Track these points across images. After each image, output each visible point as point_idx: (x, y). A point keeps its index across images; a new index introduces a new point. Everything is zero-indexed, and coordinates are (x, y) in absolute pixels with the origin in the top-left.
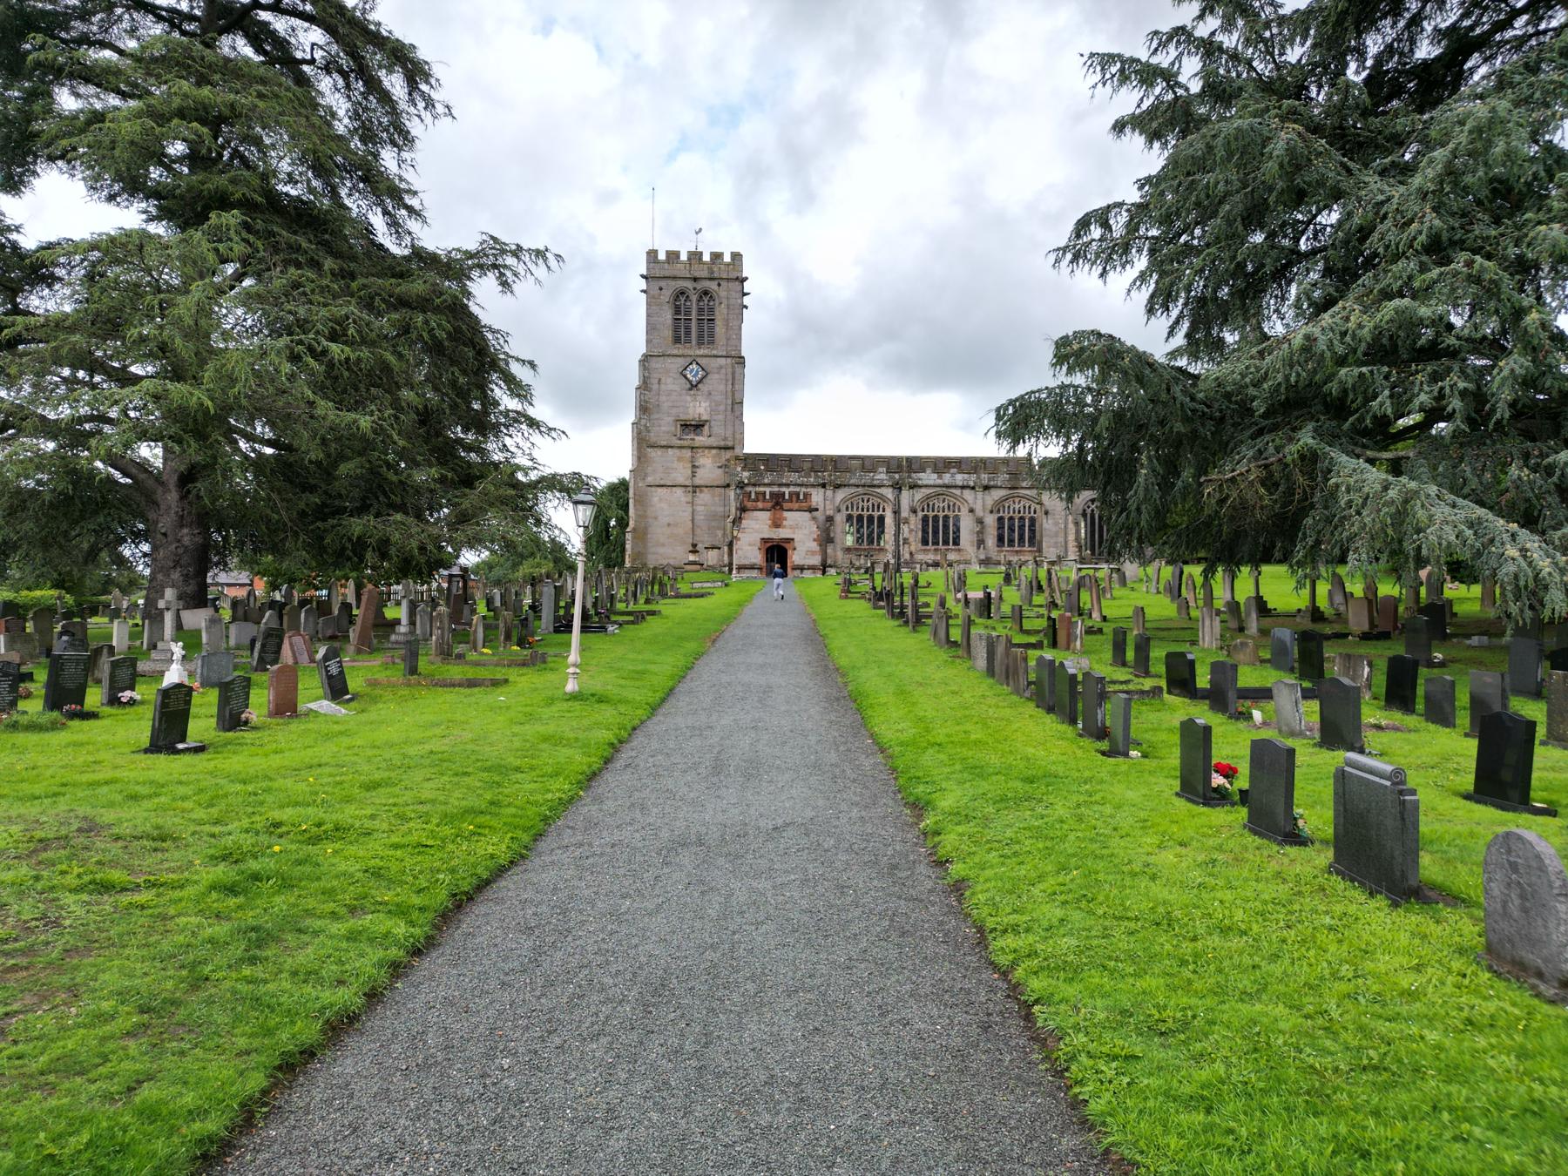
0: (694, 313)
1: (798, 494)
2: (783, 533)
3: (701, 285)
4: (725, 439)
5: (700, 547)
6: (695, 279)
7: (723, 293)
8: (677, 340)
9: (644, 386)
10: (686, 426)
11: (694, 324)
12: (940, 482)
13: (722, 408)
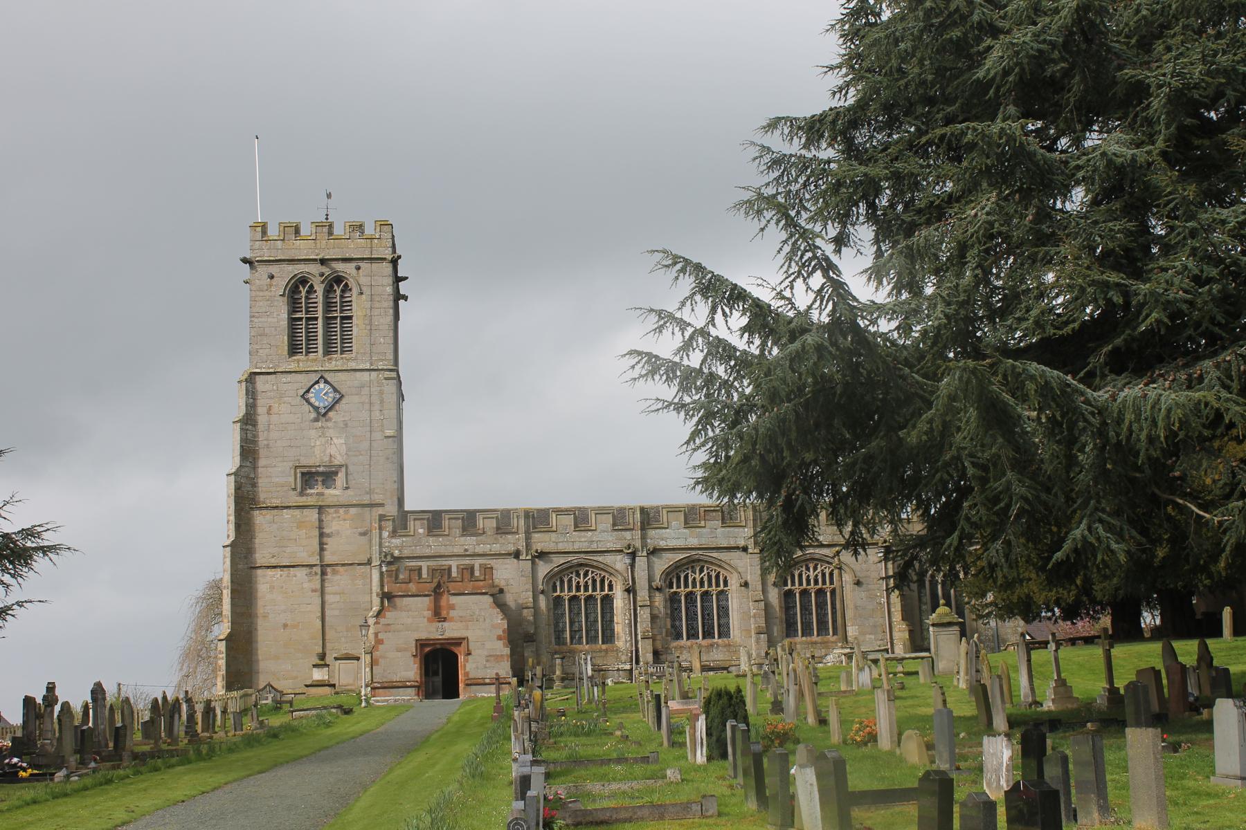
0: (320, 309)
1: (471, 569)
2: (451, 630)
3: (327, 271)
4: (370, 492)
5: (329, 659)
6: (323, 262)
7: (363, 280)
8: (293, 349)
9: (249, 421)
11: (320, 322)
12: (693, 542)
13: (366, 445)
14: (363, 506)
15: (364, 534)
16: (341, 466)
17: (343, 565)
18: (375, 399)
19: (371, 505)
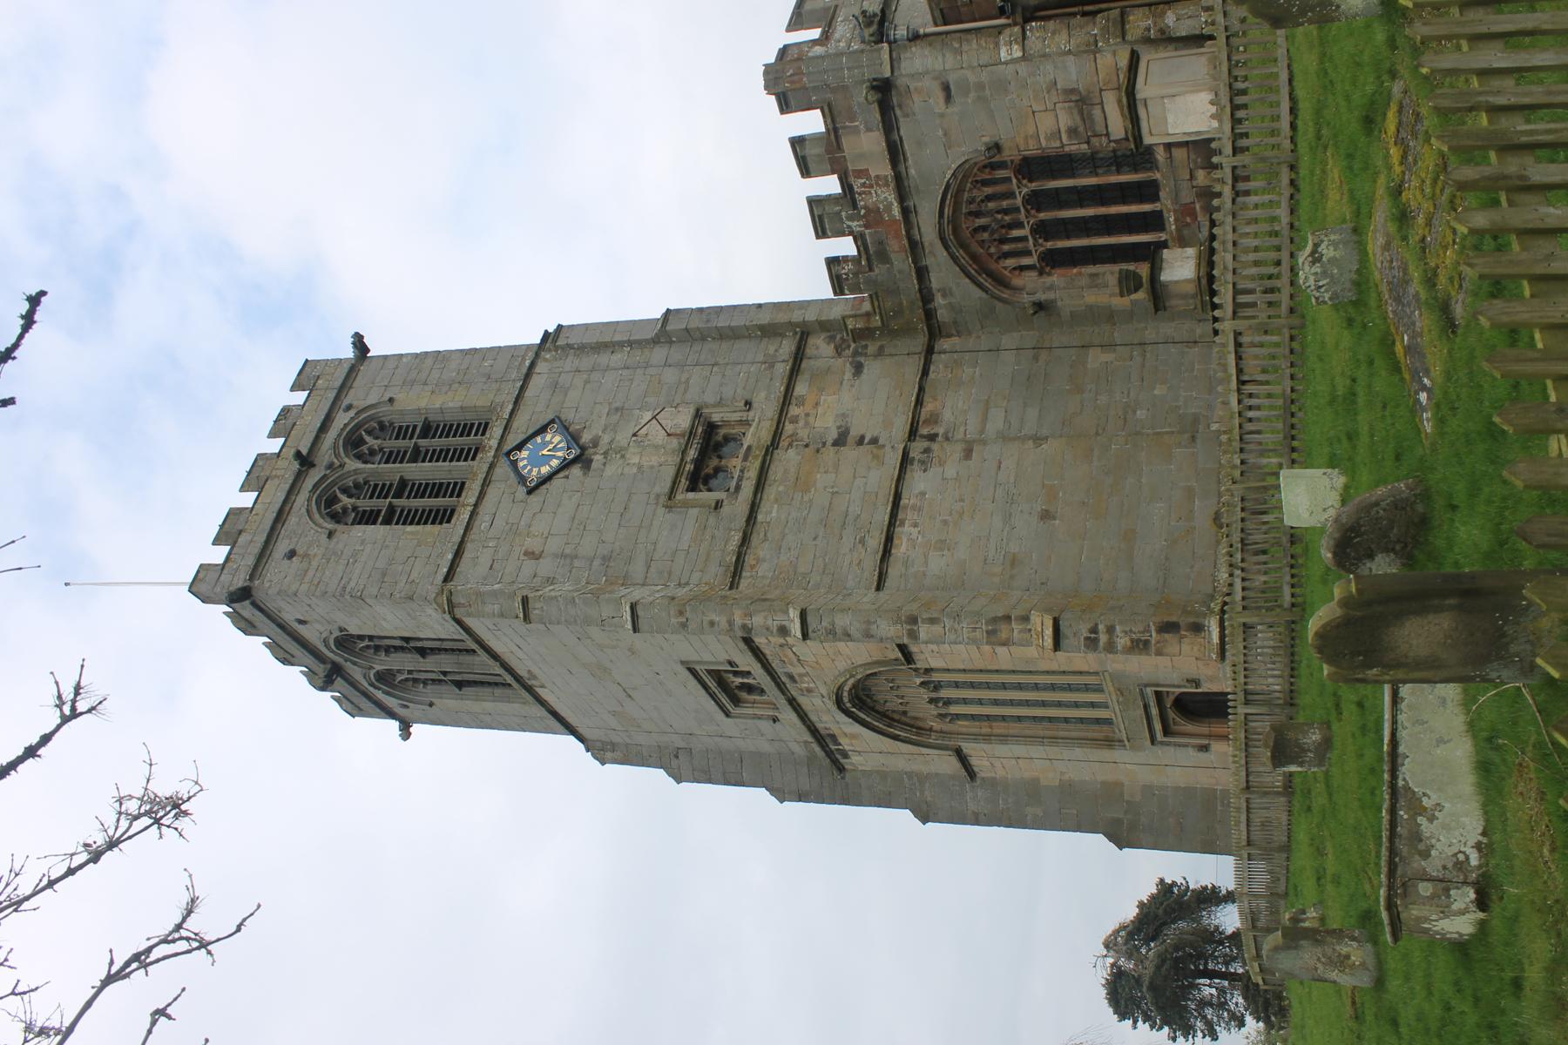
10: (698, 478)
13: (670, 376)
14: (795, 371)
15: (858, 369)
16: (698, 414)
17: (919, 402)
18: (587, 362)
19: (798, 357)
